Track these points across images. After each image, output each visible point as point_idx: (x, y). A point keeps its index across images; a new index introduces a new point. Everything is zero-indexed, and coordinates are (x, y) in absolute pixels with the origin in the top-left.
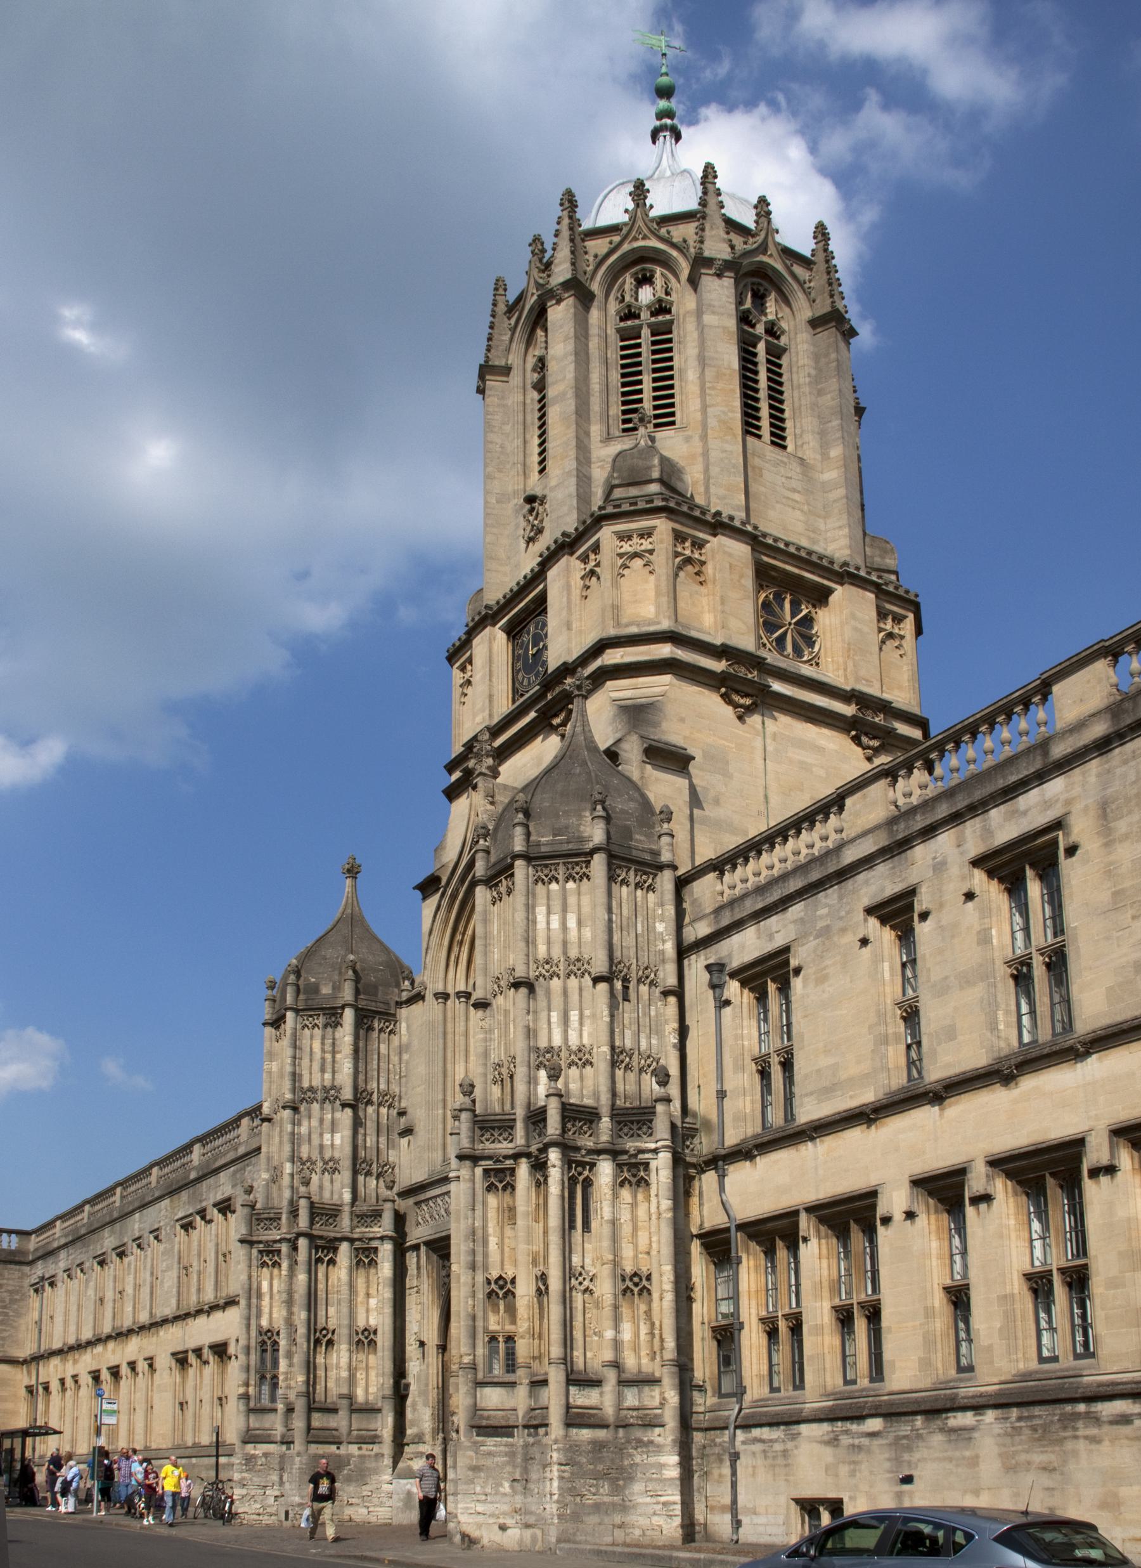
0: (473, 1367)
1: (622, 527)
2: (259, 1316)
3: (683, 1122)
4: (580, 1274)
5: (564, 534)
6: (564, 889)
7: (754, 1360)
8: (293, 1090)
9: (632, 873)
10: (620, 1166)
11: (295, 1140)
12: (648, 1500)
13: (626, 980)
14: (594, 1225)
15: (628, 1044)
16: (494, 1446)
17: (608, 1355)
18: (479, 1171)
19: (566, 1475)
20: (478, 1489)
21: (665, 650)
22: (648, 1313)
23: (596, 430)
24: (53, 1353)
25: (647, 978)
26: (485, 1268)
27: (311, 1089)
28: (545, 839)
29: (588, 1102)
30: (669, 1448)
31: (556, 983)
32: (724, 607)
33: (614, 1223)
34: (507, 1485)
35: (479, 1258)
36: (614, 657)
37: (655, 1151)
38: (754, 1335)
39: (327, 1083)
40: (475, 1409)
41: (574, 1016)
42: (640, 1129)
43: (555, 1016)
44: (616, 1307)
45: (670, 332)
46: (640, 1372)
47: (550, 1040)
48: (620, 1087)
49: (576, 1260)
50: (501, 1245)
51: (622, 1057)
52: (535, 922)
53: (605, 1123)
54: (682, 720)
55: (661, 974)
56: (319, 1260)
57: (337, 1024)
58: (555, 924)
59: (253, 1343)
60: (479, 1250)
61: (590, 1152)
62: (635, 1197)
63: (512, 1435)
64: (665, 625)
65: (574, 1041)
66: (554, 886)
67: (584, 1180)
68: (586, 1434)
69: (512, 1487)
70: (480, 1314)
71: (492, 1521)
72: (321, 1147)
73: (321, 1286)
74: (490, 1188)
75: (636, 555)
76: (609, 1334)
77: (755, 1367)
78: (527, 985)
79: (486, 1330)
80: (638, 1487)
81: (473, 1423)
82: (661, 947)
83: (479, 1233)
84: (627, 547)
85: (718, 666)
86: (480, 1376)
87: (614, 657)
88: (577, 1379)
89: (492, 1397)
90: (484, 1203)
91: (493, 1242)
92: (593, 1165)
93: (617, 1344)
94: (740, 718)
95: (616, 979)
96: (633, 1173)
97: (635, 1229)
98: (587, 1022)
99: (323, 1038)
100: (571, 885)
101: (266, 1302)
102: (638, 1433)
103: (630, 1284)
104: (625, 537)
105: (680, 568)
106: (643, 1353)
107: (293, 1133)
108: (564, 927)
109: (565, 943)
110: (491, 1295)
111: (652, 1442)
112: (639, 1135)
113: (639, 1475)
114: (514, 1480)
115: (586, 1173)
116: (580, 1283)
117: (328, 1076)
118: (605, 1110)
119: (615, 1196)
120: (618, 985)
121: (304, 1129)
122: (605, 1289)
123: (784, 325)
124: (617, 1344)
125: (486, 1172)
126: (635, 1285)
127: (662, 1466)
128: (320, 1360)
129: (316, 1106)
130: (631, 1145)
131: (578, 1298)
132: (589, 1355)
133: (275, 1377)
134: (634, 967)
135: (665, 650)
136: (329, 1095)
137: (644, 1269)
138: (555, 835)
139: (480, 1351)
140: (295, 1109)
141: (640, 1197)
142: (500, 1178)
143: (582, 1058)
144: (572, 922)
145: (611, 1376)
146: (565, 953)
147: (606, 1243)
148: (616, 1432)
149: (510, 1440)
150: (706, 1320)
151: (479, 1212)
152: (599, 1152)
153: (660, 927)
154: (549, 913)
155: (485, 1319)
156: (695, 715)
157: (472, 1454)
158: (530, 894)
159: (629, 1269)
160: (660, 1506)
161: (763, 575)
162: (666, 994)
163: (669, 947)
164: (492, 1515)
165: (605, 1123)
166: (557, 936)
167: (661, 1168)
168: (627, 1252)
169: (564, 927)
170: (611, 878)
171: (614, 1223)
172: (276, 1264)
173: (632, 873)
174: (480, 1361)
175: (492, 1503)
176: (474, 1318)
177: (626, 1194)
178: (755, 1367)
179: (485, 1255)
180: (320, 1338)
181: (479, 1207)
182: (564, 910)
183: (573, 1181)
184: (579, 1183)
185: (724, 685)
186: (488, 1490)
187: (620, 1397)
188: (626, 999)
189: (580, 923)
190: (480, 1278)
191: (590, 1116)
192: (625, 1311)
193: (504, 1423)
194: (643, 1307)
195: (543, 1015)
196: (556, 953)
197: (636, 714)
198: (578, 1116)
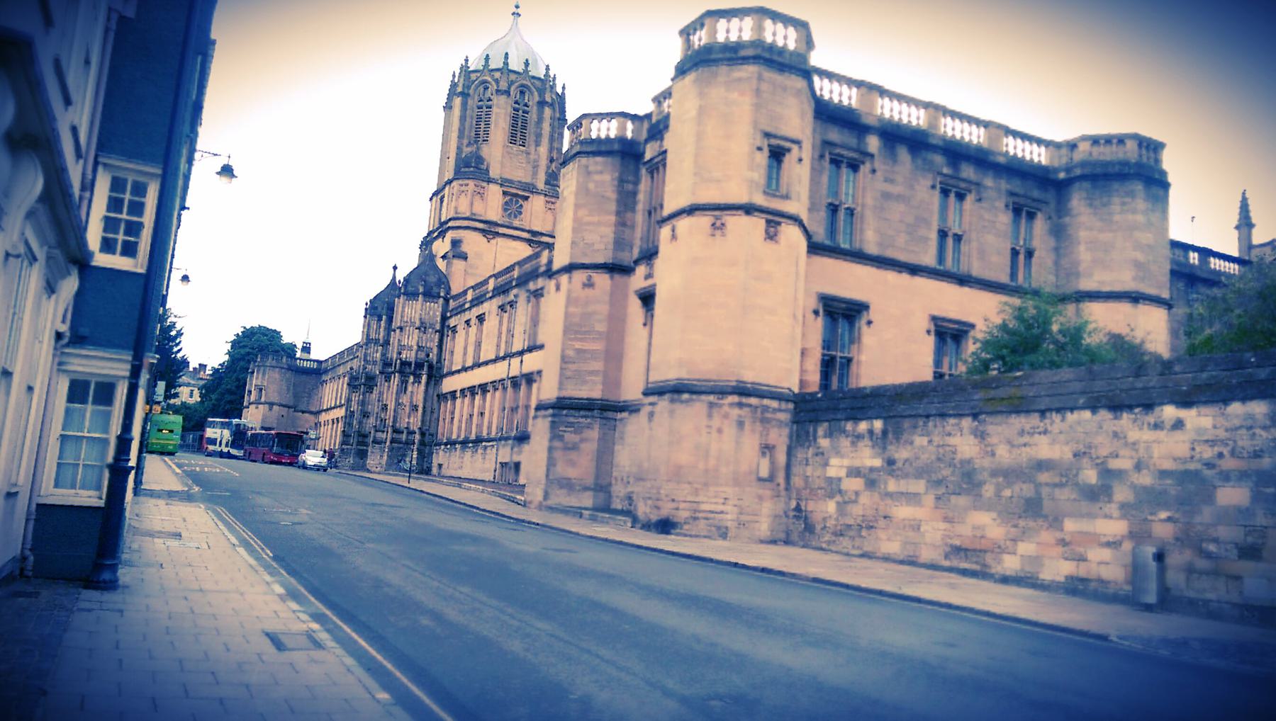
21: (465, 223)
25: (432, 326)
28: (410, 289)
32: (492, 205)
36: (450, 224)
64: (468, 214)
68: (395, 445)
78: (401, 328)
85: (481, 226)
87: (450, 224)
88: (396, 431)
89: (379, 435)
95: (423, 327)
96: (418, 378)
122: (407, 409)
126: (414, 408)
135: (465, 223)
136: (376, 341)
142: (388, 379)
143: (410, 348)
156: (473, 242)
161: (505, 193)
167: (424, 378)
180: (366, 415)
184: (404, 383)
191: (410, 364)
197: (456, 243)
198: (405, 364)
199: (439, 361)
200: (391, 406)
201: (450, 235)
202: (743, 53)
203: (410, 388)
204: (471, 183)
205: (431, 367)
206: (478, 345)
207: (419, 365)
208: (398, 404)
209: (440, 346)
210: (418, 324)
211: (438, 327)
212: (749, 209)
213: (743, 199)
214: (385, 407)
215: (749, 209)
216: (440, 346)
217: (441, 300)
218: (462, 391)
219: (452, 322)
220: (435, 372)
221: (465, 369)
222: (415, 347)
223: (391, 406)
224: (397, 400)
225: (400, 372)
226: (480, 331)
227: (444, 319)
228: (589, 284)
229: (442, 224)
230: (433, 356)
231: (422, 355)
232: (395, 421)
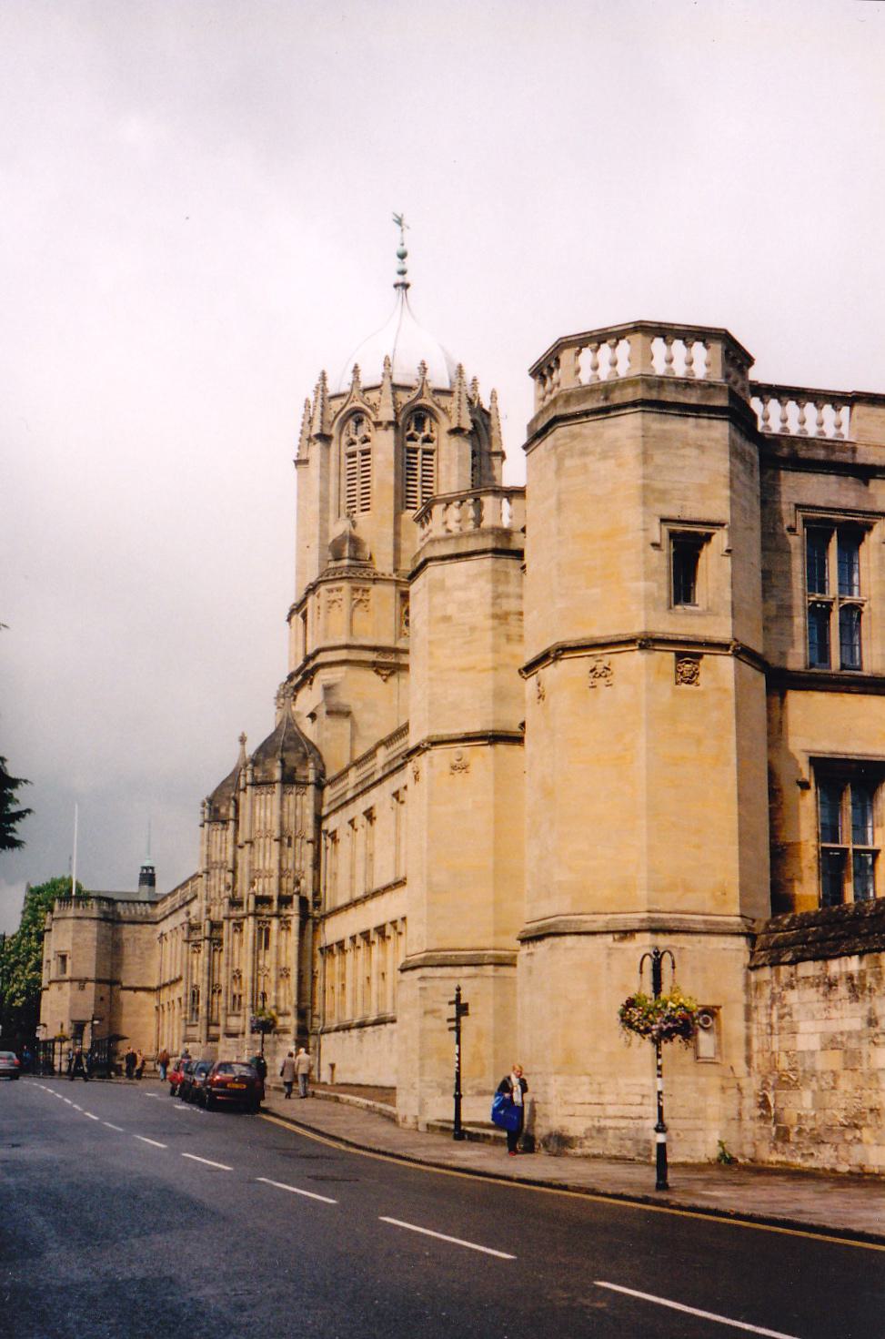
1: (329, 586)
2: (192, 978)
6: (266, 799)
8: (208, 863)
9: (295, 788)
11: (208, 889)
13: (290, 838)
14: (270, 946)
18: (231, 924)
22: (289, 985)
23: (332, 516)
24: (165, 985)
26: (233, 965)
27: (216, 862)
29: (271, 894)
31: (262, 840)
35: (230, 961)
39: (223, 859)
41: (268, 855)
43: (261, 855)
44: (277, 982)
45: (369, 453)
49: (261, 962)
52: (255, 813)
56: (215, 950)
57: (227, 829)
58: (262, 814)
59: (189, 993)
60: (230, 957)
61: (268, 916)
65: (267, 868)
66: (263, 796)
72: (220, 892)
73: (216, 963)
74: (236, 931)
75: (334, 601)
78: (251, 842)
79: (232, 992)
86: (229, 1013)
90: (233, 937)
91: (236, 953)
92: (270, 922)
93: (277, 999)
94: (385, 681)
96: (285, 925)
99: (221, 836)
100: (269, 796)
101: (195, 971)
104: (331, 591)
105: (355, 606)
107: (207, 886)
108: (265, 815)
109: (265, 824)
110: (234, 977)
117: (223, 855)
118: (275, 898)
120: (286, 841)
121: (212, 883)
122: (273, 975)
123: (434, 435)
124: (277, 999)
125: (234, 924)
128: (215, 1000)
129: (217, 871)
130: (284, 912)
131: (261, 979)
133: (198, 1010)
135: (342, 655)
136: (222, 866)
140: (208, 873)
142: (238, 927)
144: (268, 814)
146: (265, 828)
147: (274, 955)
151: (231, 942)
154: (260, 809)
155: (231, 987)
158: (253, 801)
159: (283, 966)
162: (308, 842)
163: (310, 821)
165: (275, 903)
167: (295, 925)
169: (265, 815)
170: (283, 793)
172: (199, 952)
173: (295, 788)
176: (227, 987)
177: (283, 933)
179: (232, 960)
180: (214, 989)
181: (231, 939)
182: (266, 808)
183: (260, 929)
185: (376, 667)
188: (289, 845)
192: (282, 984)
195: (256, 854)
196: (262, 828)
197: (328, 689)
198: (262, 900)
199: (316, 893)
200: (247, 974)
201: (323, 677)
202: (617, 398)
203: (273, 942)
204: (345, 585)
205: (303, 901)
206: (370, 857)
209: (316, 864)
210: (276, 834)
211: (310, 835)
212: (648, 643)
213: (637, 628)
214: (237, 976)
215: (648, 643)
216: (316, 864)
217: (311, 789)
218: (353, 938)
219: (329, 825)
220: (312, 914)
221: (354, 903)
222: (276, 873)
223: (247, 974)
226: (370, 836)
227: (319, 819)
228: (459, 767)
229: (308, 659)
230: (307, 886)
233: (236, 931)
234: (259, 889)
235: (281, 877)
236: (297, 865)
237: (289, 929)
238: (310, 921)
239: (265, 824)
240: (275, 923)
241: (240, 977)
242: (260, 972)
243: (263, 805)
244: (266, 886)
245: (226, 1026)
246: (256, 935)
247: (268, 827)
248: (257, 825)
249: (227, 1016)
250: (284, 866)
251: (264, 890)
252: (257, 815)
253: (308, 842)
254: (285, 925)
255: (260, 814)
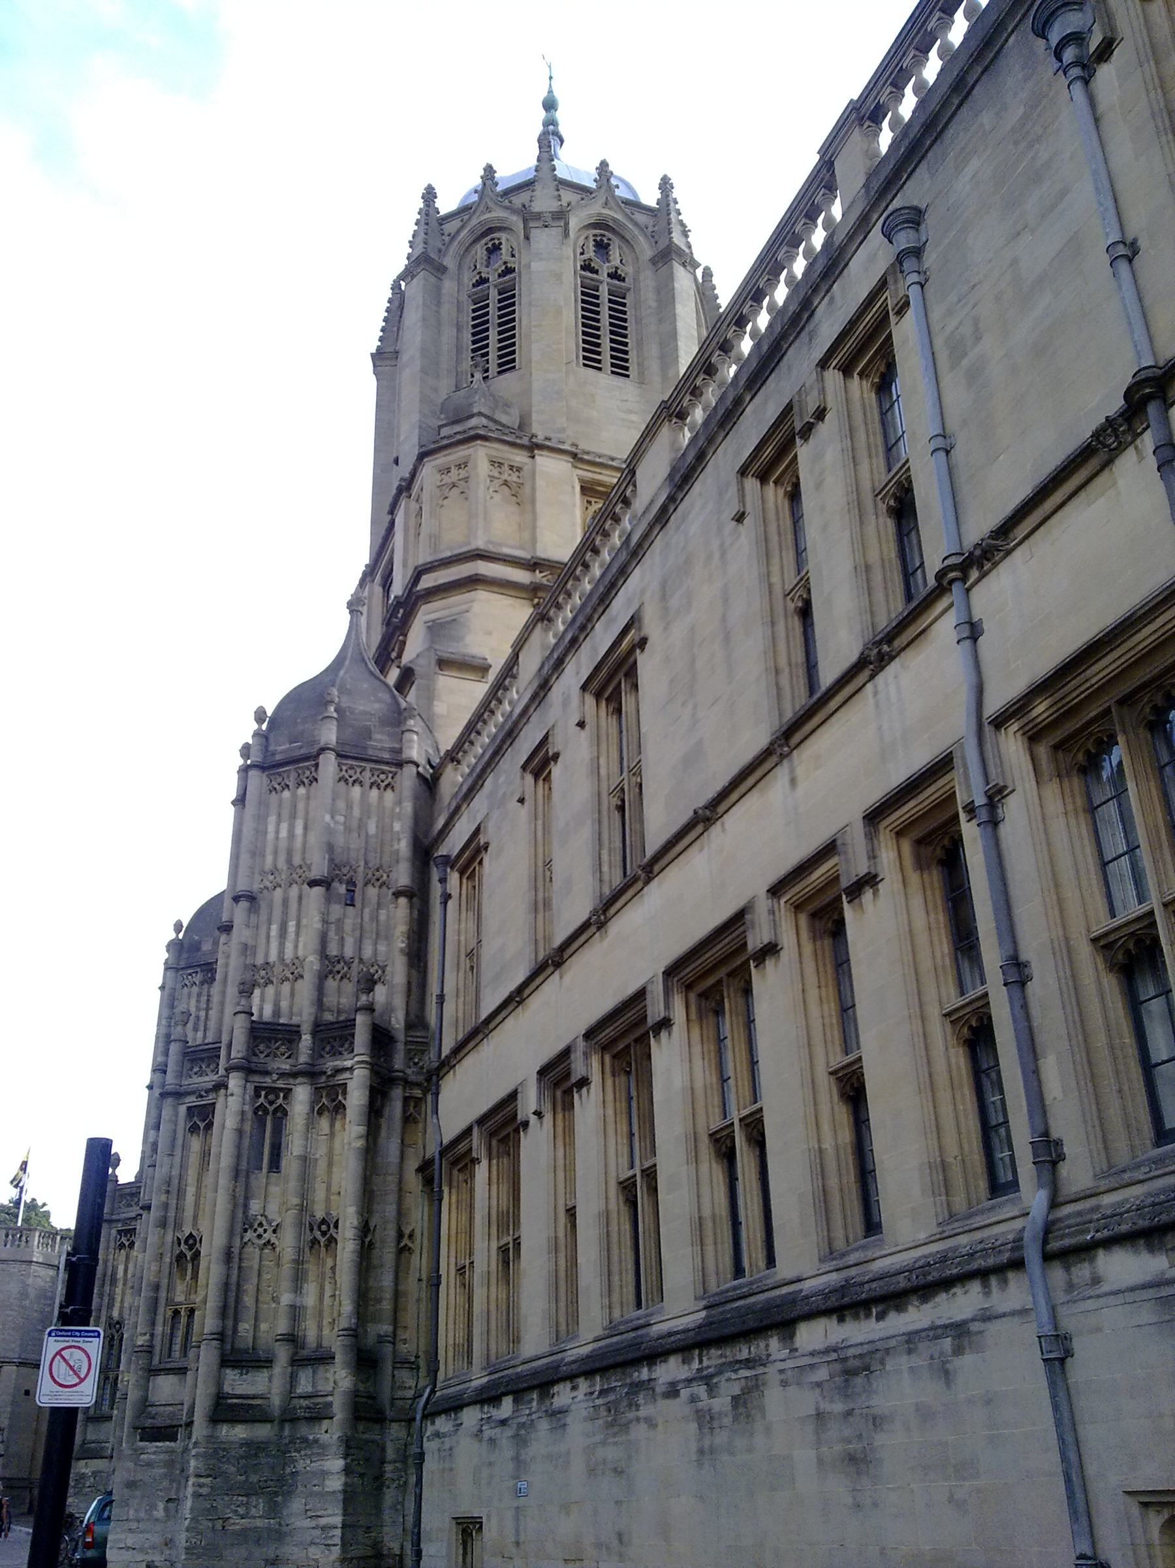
0: (149, 1350)
3: (406, 1036)
4: (261, 1225)
5: (402, 479)
6: (294, 796)
7: (451, 1326)
10: (317, 1091)
12: (308, 1523)
13: (351, 883)
14: (284, 1163)
15: (349, 952)
16: (155, 1453)
17: (282, 1327)
18: (183, 1110)
19: (204, 1491)
20: (131, 1512)
25: (378, 878)
26: (178, 1225)
29: (295, 1020)
30: (334, 1449)
33: (306, 1160)
34: (161, 1505)
35: (171, 1214)
36: (427, 582)
37: (351, 1069)
38: (452, 1291)
40: (144, 1404)
42: (342, 1046)
44: (298, 1262)
46: (320, 1346)
47: (267, 955)
48: (330, 1000)
49: (255, 1207)
50: (198, 1196)
51: (338, 967)
53: (306, 1039)
54: (489, 633)
55: (393, 875)
58: (284, 833)
61: (283, 1075)
62: (332, 1126)
63: (173, 1438)
67: (275, 1111)
68: (240, 1432)
69: (166, 1510)
70: (164, 1282)
71: (140, 1557)
74: (194, 1129)
76: (286, 1298)
77: (451, 1334)
79: (169, 1301)
80: (297, 1504)
81: (137, 1424)
82: (396, 847)
83: (175, 1182)
84: (447, 479)
87: (427, 582)
88: (238, 1358)
89: (165, 1388)
91: (191, 1191)
92: (288, 1092)
93: (296, 1313)
96: (329, 1101)
97: (330, 1165)
98: (303, 932)
100: (302, 791)
102: (304, 1430)
103: (318, 1234)
106: (325, 1322)
108: (291, 835)
110: (181, 1257)
111: (316, 1441)
112: (341, 1054)
113: (300, 1488)
114: (170, 1500)
115: (280, 1101)
116: (260, 1236)
119: (310, 1125)
124: (296, 1313)
126: (319, 1234)
127: (324, 1474)
130: (330, 1064)
131: (253, 1253)
132: (263, 1327)
134: (361, 869)
137: (334, 1213)
138: (291, 743)
139: (159, 1329)
141: (338, 1125)
144: (299, 830)
145: (282, 1354)
146: (289, 861)
147: (293, 1184)
148: (282, 1429)
149: (173, 1444)
150: (424, 1277)
152: (295, 1075)
153: (397, 827)
155: (170, 1288)
157: (131, 1465)
159: (320, 1215)
160: (319, 1532)
163: (404, 846)
164: (142, 1550)
165: (306, 1039)
166: (283, 845)
168: (320, 1194)
169: (291, 835)
171: (306, 1160)
174: (157, 1342)
175: (141, 1532)
177: (324, 1123)
178: (451, 1334)
179: (179, 1209)
181: (178, 1152)
182: (293, 816)
183: (260, 1113)
184: (268, 1113)
186: (142, 1515)
187: (293, 1380)
189: (306, 828)
190: (169, 1238)
191: (291, 1034)
192: (312, 1269)
193: (169, 1422)
194: (329, 1262)
196: (282, 864)
198: (268, 1035)
199: (416, 1021)
203: (294, 1144)
205: (381, 1038)
207: (333, 1034)
208: (243, 1222)
209: (417, 955)
211: (402, 876)
214: (187, 1256)
216: (417, 955)
220: (405, 1070)
222: (312, 962)
224: (240, 1202)
225: (248, 1069)
230: (390, 995)
231: (342, 995)
232: (230, 1309)
233: (194, 1129)
234: (263, 1005)
235: (322, 978)
236: (368, 952)
237: (340, 1108)
238: (397, 1093)
239: (290, 852)
240: (302, 1094)
241: (197, 1255)
242: (249, 1235)
243: (285, 813)
244: (284, 1004)
245: (144, 1404)
246: (248, 1127)
247: (297, 861)
248: (269, 859)
249: (153, 1372)
250: (333, 950)
251: (277, 1012)
252: (271, 836)
253: (397, 894)
254: (329, 1101)
255: (277, 832)
